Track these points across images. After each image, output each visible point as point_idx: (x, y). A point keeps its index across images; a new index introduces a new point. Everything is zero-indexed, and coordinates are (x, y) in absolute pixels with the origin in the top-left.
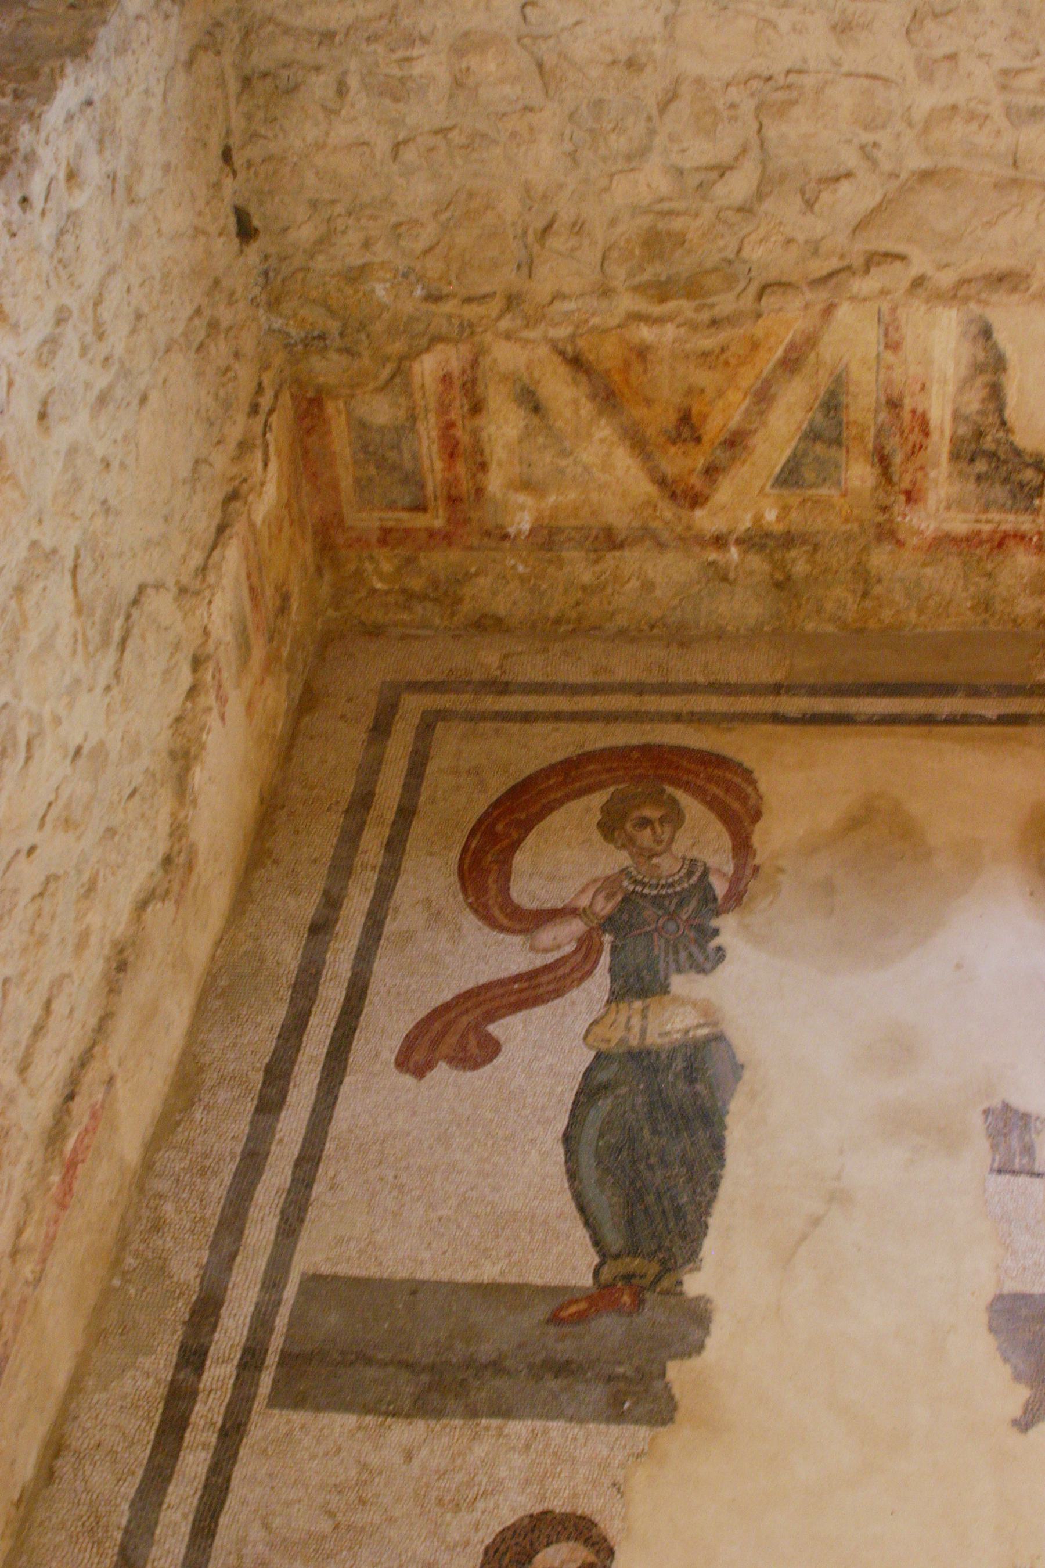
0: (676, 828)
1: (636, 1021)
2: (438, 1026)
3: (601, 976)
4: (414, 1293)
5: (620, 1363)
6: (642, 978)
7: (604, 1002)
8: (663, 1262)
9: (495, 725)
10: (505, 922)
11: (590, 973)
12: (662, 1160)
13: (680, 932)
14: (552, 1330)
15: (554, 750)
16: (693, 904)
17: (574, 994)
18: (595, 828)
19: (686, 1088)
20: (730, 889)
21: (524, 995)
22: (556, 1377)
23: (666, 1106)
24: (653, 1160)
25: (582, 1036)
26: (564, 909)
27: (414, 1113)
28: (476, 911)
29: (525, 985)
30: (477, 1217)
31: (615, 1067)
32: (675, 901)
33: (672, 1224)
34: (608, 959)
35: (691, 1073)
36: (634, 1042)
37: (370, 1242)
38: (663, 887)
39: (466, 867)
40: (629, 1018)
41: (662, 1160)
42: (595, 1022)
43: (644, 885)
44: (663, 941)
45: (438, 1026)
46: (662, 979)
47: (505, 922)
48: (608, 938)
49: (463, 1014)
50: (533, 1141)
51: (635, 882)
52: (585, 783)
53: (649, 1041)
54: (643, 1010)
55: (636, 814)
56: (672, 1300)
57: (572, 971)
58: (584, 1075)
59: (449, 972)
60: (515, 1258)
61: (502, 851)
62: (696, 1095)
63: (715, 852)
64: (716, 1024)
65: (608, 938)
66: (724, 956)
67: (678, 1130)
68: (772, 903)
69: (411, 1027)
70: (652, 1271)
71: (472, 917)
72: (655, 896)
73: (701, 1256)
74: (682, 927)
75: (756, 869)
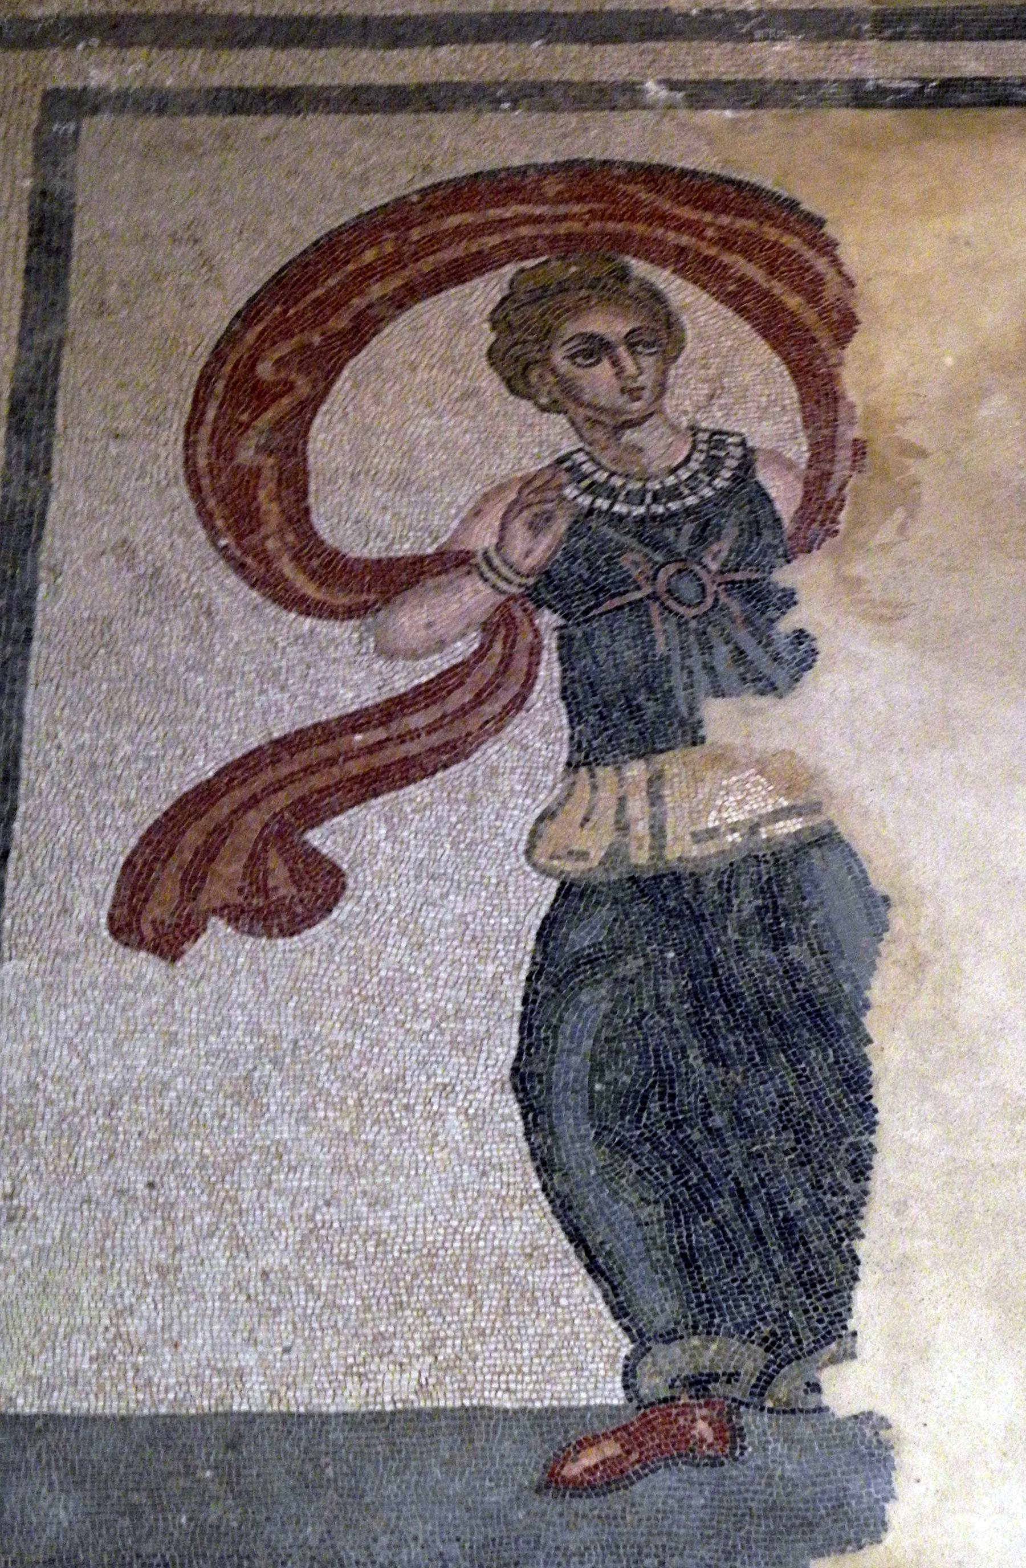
0: (668, 360)
1: (637, 807)
2: (193, 838)
3: (546, 708)
4: (232, 1446)
6: (639, 708)
7: (561, 769)
8: (770, 1344)
9: (222, 122)
10: (311, 590)
11: (519, 702)
12: (738, 1119)
14: (551, 1506)
15: (363, 180)
16: (731, 532)
17: (491, 751)
18: (485, 363)
19: (769, 955)
20: (807, 497)
21: (379, 760)
23: (732, 999)
24: (718, 1121)
25: (522, 847)
26: (440, 554)
28: (240, 568)
29: (381, 734)
30: (349, 1265)
31: (604, 913)
32: (688, 528)
33: (778, 1260)
35: (777, 919)
36: (641, 857)
37: (118, 1335)
38: (656, 498)
39: (202, 462)
40: (622, 802)
41: (738, 1119)
42: (547, 816)
43: (613, 494)
44: (671, 626)
45: (193, 838)
46: (684, 710)
47: (311, 590)
48: (548, 620)
49: (246, 806)
50: (445, 1089)
51: (592, 489)
52: (447, 255)
53: (673, 852)
54: (650, 782)
55: (571, 329)
56: (803, 1429)
57: (479, 699)
58: (539, 935)
59: (202, 709)
60: (447, 1352)
61: (278, 425)
62: (792, 972)
63: (763, 413)
64: (816, 808)
65: (548, 620)
66: (814, 652)
67: (762, 1048)
68: (902, 528)
69: (133, 842)
70: (749, 1365)
71: (232, 580)
72: (642, 520)
73: (852, 1324)
74: (711, 589)
75: (859, 449)
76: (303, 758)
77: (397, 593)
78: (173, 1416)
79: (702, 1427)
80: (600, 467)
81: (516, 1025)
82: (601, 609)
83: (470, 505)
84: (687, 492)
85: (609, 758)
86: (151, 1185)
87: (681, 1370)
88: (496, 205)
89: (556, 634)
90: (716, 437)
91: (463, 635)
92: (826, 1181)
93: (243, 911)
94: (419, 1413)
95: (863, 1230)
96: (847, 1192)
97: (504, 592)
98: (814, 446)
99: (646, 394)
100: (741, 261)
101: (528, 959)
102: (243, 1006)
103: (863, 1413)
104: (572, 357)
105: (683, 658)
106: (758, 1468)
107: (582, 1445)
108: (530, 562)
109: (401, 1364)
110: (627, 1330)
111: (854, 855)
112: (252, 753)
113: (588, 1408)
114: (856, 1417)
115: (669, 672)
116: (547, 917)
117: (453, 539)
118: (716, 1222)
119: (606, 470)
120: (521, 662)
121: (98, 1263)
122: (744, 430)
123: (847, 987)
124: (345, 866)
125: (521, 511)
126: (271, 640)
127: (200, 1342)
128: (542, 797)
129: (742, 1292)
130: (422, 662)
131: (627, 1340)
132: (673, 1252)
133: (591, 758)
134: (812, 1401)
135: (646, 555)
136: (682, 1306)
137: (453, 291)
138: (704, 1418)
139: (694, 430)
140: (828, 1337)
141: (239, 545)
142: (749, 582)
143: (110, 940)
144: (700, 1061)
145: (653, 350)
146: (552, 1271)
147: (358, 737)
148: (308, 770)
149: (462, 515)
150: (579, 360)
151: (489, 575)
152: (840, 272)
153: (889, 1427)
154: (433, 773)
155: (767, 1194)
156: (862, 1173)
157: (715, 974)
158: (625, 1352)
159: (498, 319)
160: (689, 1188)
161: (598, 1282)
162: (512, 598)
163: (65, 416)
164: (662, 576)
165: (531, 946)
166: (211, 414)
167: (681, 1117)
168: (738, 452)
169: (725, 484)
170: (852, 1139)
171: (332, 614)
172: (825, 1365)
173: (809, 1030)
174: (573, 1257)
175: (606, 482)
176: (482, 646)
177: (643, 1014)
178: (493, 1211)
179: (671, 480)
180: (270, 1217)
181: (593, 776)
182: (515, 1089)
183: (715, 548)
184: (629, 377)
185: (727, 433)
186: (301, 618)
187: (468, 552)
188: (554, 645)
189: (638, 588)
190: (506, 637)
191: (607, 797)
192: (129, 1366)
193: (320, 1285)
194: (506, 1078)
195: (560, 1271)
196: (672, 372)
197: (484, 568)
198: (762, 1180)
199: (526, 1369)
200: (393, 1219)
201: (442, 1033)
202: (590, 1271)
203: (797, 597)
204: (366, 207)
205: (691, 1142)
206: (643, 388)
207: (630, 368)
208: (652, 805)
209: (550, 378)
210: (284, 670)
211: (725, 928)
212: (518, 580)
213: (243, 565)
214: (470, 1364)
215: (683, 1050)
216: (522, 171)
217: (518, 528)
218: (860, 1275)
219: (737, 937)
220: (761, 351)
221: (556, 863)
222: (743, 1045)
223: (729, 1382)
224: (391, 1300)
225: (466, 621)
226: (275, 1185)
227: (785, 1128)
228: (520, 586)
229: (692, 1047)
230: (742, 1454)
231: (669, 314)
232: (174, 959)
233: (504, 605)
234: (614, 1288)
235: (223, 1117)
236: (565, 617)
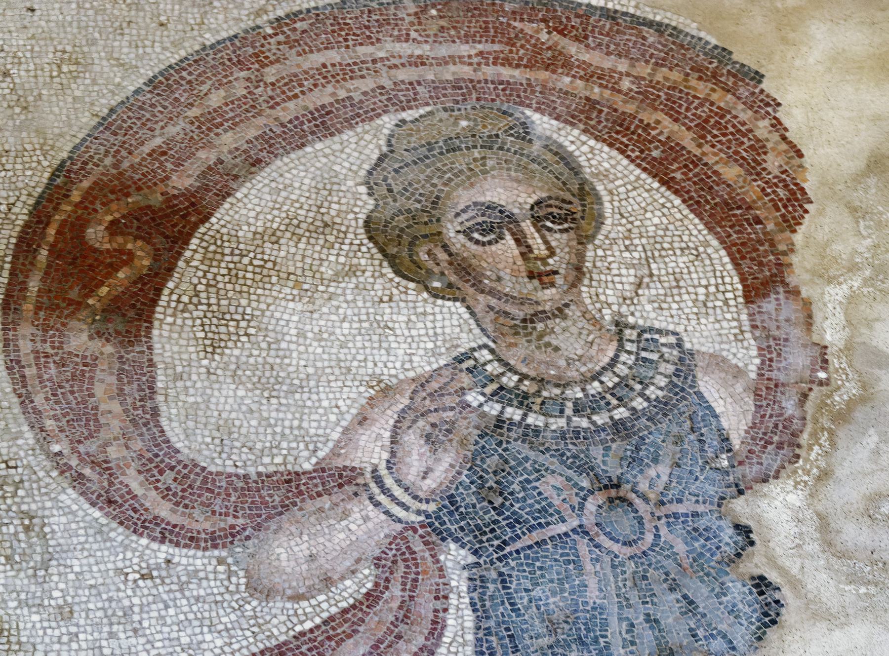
10: (164, 510)
13: (649, 538)
28: (79, 480)
47: (164, 510)
51: (501, 394)
55: (464, 197)
71: (70, 497)
77: (269, 518)
80: (512, 370)
82: (519, 545)
83: (354, 411)
84: (614, 402)
88: (369, 40)
89: (466, 574)
90: (647, 336)
97: (400, 521)
99: (559, 280)
104: (467, 233)
108: (430, 483)
115: (605, 625)
117: (335, 453)
119: (516, 373)
120: (425, 606)
122: (680, 329)
126: (119, 571)
135: (569, 479)
137: (319, 146)
139: (620, 326)
141: (74, 450)
142: (695, 515)
145: (566, 226)
149: (344, 423)
150: (476, 235)
151: (382, 498)
152: (784, 138)
164: (591, 505)
169: (660, 393)
171: (193, 541)
175: (517, 387)
176: (377, 584)
179: (595, 387)
183: (652, 473)
184: (536, 258)
185: (659, 331)
186: (155, 546)
187: (353, 469)
189: (564, 521)
196: (590, 254)
197: (375, 490)
206: (556, 273)
207: (539, 248)
209: (442, 256)
210: (136, 609)
212: (415, 505)
217: (412, 439)
225: (356, 555)
228: (418, 512)
231: (583, 183)
233: (401, 535)
236: (475, 553)
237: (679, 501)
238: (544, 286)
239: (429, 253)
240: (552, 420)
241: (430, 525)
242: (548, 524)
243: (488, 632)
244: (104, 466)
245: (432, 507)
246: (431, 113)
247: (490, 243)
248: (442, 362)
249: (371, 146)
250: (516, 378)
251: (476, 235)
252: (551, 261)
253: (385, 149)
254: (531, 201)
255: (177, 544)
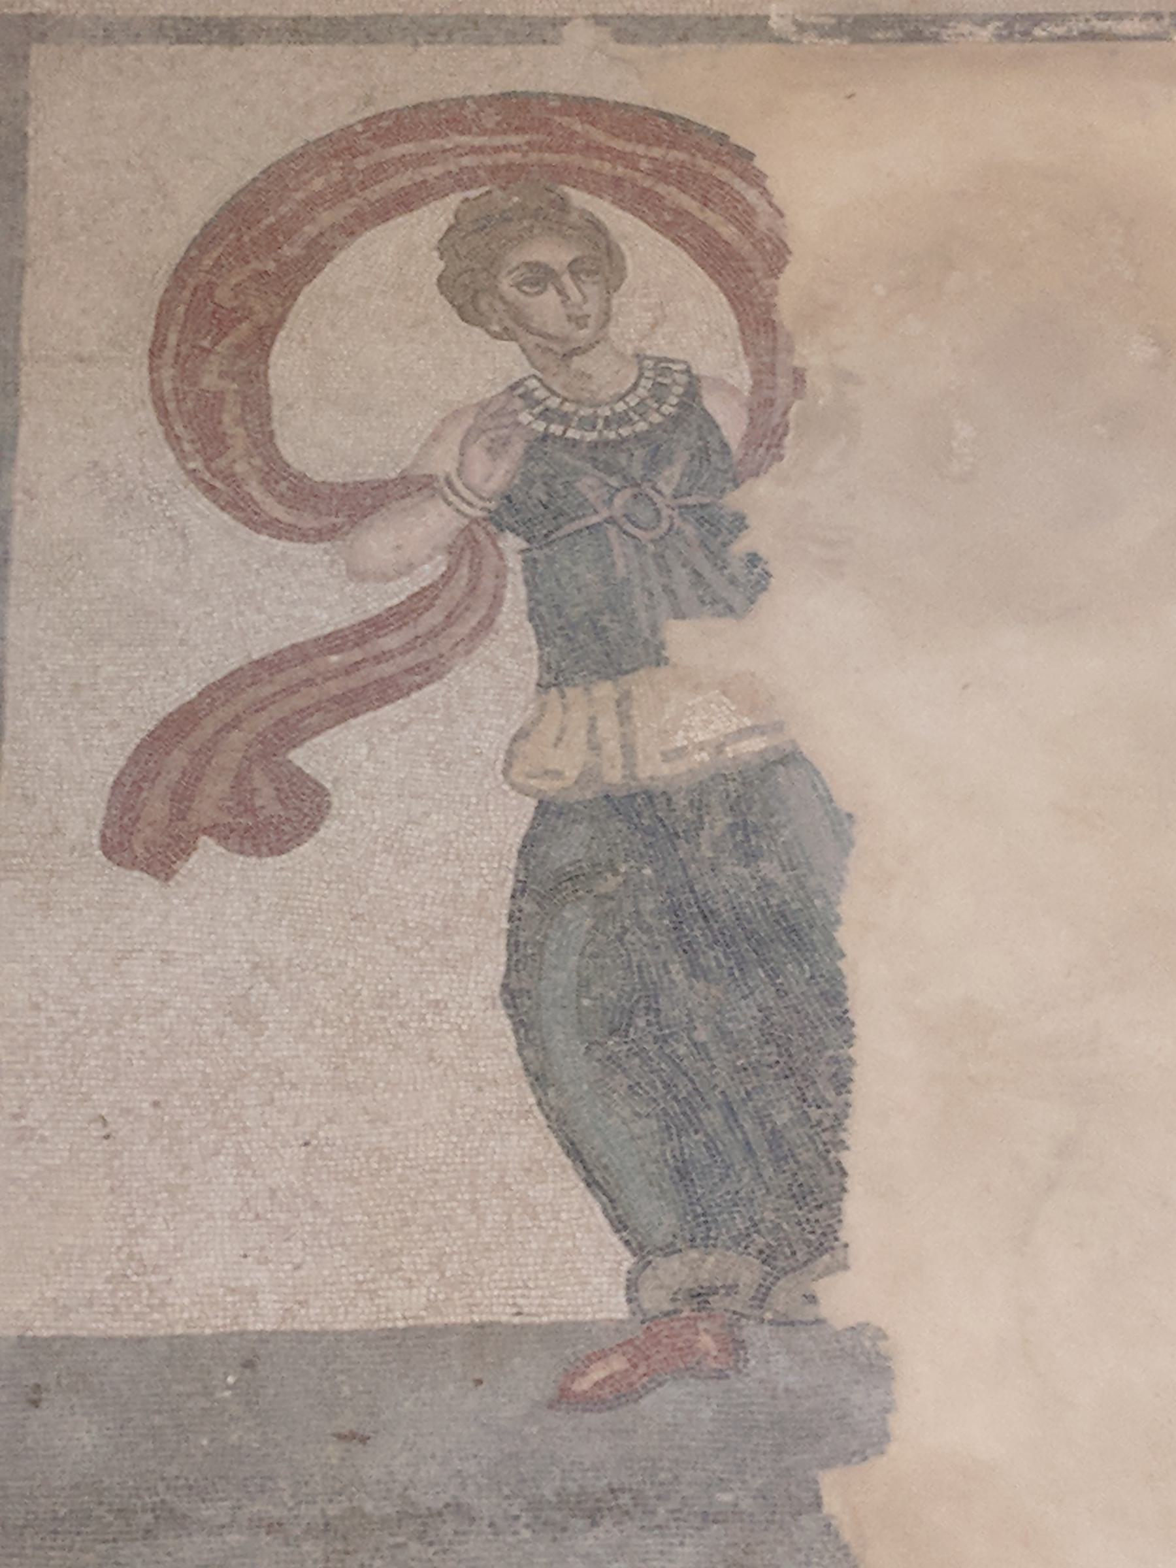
1: (608, 725)
5: (723, 1484)
7: (532, 687)
8: (766, 1257)
10: (278, 512)
11: (487, 624)
12: (723, 1034)
21: (354, 682)
22: (594, 1524)
24: (701, 1035)
25: (499, 766)
26: (403, 478)
27: (167, 959)
28: (209, 489)
29: (357, 655)
30: (356, 1182)
33: (768, 1172)
34: (523, 591)
35: (747, 839)
36: (614, 775)
39: (168, 386)
42: (522, 735)
43: (565, 419)
47: (278, 512)
51: (546, 415)
55: (515, 258)
57: (450, 618)
62: (766, 885)
64: (779, 727)
65: (511, 543)
67: (741, 965)
69: (122, 762)
72: (594, 446)
73: (844, 1236)
74: (666, 512)
76: (281, 679)
78: (189, 1337)
79: (706, 1342)
80: (553, 393)
81: (503, 941)
83: (430, 430)
84: (636, 418)
85: (577, 679)
86: (156, 1104)
87: (683, 1282)
88: (438, 135)
89: (520, 557)
90: (663, 365)
91: (430, 558)
92: (810, 1095)
93: (232, 831)
94: (432, 1330)
95: (848, 1143)
96: (829, 1105)
97: (466, 516)
98: (755, 372)
99: (591, 322)
100: (674, 190)
101: (511, 876)
102: (236, 925)
103: (859, 1324)
104: (518, 286)
105: (643, 580)
106: (761, 1381)
107: (590, 1360)
108: (493, 486)
109: (410, 1280)
110: (627, 1243)
111: (818, 773)
112: (232, 674)
113: (593, 1322)
114: (853, 1328)
116: (526, 836)
117: (415, 465)
118: (707, 1135)
119: (558, 396)
120: (488, 582)
121: (108, 1182)
122: (688, 358)
123: (817, 902)
124: (328, 786)
125: (478, 437)
126: (244, 562)
127: (212, 1260)
128: (515, 717)
129: (736, 1205)
130: (391, 584)
131: (628, 1254)
132: (668, 1166)
133: (561, 679)
134: (809, 1313)
135: (601, 480)
136: (679, 1220)
137: (400, 219)
138: (706, 1330)
139: (639, 357)
140: (821, 1249)
141: (208, 468)
142: (702, 506)
143: (104, 859)
144: (681, 976)
146: (551, 1186)
147: (334, 658)
148: (289, 691)
151: (452, 498)
152: (771, 204)
153: (885, 1337)
154: (408, 694)
155: (755, 1107)
156: (844, 1085)
157: (692, 891)
158: (626, 1265)
159: (442, 248)
160: (678, 1101)
161: (595, 1196)
162: (475, 521)
163: (31, 339)
164: (618, 501)
165: (513, 864)
166: (173, 339)
167: (667, 1031)
168: (683, 379)
169: (672, 409)
170: (830, 1052)
171: (304, 537)
172: (820, 1277)
173: (785, 946)
174: (571, 1172)
176: (449, 568)
177: (625, 930)
178: (490, 1126)
179: (620, 407)
180: (274, 1134)
181: (563, 697)
182: (507, 1006)
184: (573, 305)
185: (673, 361)
186: (274, 541)
187: (431, 476)
188: (518, 568)
189: (596, 512)
190: (472, 561)
191: (578, 717)
192: (143, 1286)
193: (326, 1202)
194: (496, 994)
195: (559, 1186)
196: (615, 302)
197: (446, 490)
198: (747, 1093)
199: (531, 1284)
200: (395, 1135)
201: (432, 948)
202: (588, 1185)
203: (747, 522)
204: (312, 136)
205: (678, 1057)
206: (589, 316)
208: (622, 724)
209: (499, 306)
211: (698, 845)
212: (481, 504)
213: (213, 487)
214: (477, 1279)
215: (665, 964)
216: (461, 102)
218: (848, 1186)
219: (710, 854)
220: (700, 278)
221: (532, 782)
222: (723, 960)
223: (728, 1294)
224: (397, 1216)
226: (278, 1103)
227: (767, 1043)
228: (482, 509)
229: (674, 962)
230: (745, 1366)
232: (167, 879)
233: (467, 528)
234: (611, 1201)
235: (222, 1035)
236: (528, 541)
237: (690, 495)
238: (581, 327)
239: (490, 305)
240: (586, 434)
241: (491, 519)
242: (584, 515)
243: (539, 603)
244: (229, 477)
245: (492, 505)
246: (488, 192)
247: (537, 293)
248: (500, 390)
249: (442, 219)
250: (558, 400)
251: (525, 288)
252: (585, 307)
253: (453, 221)
254: (570, 259)
255: (291, 540)
